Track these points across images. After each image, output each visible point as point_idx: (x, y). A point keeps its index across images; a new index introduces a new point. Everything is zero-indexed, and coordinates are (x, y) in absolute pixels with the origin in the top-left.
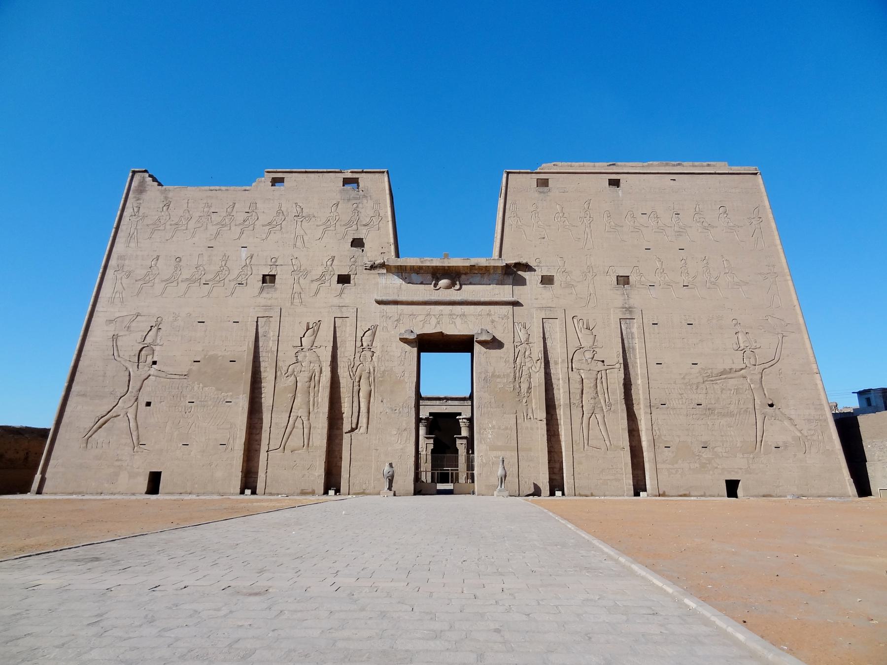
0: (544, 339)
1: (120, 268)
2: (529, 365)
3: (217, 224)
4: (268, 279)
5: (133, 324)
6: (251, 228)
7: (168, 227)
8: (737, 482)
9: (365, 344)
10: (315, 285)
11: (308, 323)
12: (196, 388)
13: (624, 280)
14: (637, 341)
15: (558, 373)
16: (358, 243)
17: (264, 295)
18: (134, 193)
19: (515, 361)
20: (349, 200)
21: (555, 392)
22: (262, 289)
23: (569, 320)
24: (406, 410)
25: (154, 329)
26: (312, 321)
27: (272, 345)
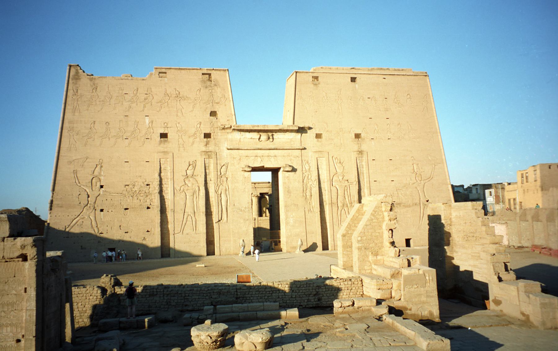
0: (318, 168)
1: (71, 129)
2: (310, 183)
3: (129, 101)
4: (164, 136)
5: (85, 164)
6: (150, 104)
7: (98, 103)
8: (410, 239)
9: (222, 173)
10: (191, 140)
11: (189, 162)
12: (129, 201)
13: (357, 136)
14: (365, 169)
15: (325, 186)
16: (213, 114)
17: (162, 145)
18: (72, 80)
19: (303, 182)
20: (206, 87)
21: (324, 197)
22: (161, 142)
23: (331, 158)
24: (247, 210)
25: (99, 167)
26: (192, 160)
27: (169, 175)
